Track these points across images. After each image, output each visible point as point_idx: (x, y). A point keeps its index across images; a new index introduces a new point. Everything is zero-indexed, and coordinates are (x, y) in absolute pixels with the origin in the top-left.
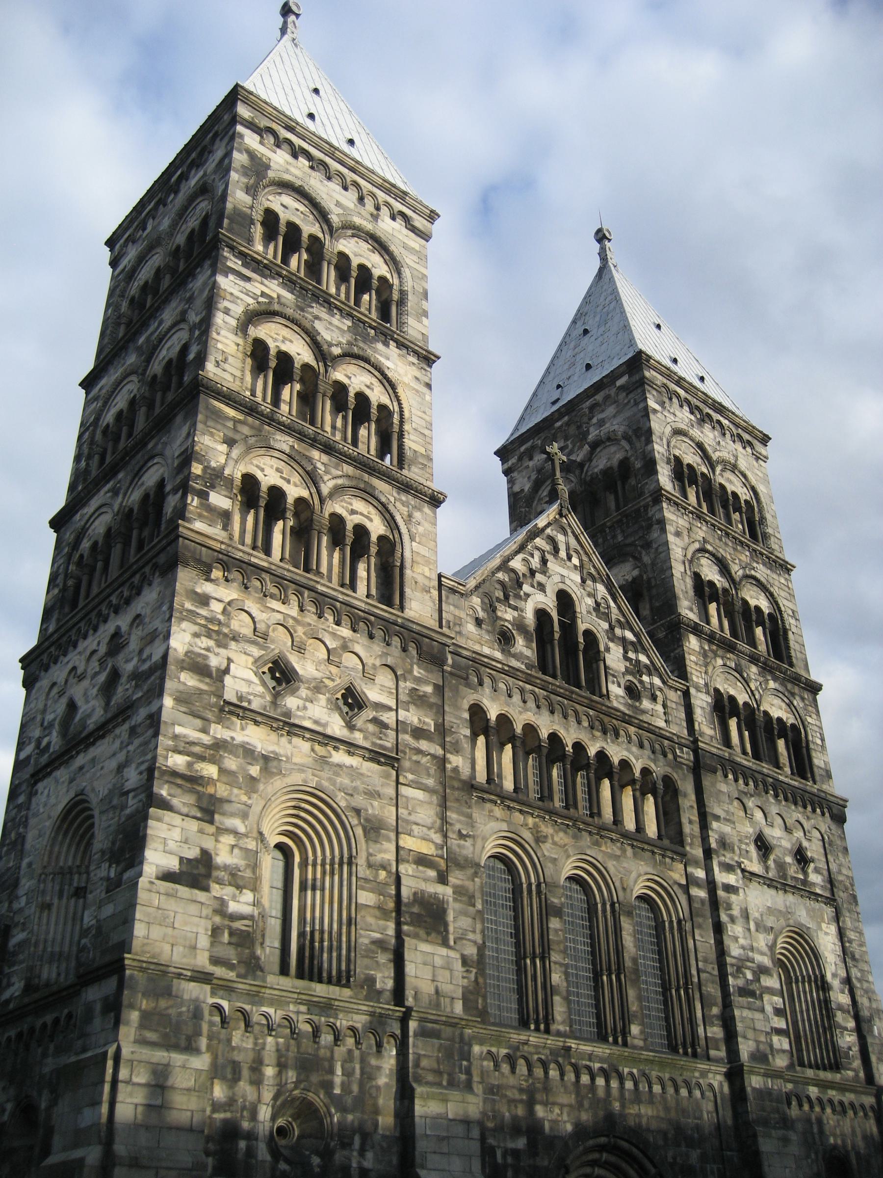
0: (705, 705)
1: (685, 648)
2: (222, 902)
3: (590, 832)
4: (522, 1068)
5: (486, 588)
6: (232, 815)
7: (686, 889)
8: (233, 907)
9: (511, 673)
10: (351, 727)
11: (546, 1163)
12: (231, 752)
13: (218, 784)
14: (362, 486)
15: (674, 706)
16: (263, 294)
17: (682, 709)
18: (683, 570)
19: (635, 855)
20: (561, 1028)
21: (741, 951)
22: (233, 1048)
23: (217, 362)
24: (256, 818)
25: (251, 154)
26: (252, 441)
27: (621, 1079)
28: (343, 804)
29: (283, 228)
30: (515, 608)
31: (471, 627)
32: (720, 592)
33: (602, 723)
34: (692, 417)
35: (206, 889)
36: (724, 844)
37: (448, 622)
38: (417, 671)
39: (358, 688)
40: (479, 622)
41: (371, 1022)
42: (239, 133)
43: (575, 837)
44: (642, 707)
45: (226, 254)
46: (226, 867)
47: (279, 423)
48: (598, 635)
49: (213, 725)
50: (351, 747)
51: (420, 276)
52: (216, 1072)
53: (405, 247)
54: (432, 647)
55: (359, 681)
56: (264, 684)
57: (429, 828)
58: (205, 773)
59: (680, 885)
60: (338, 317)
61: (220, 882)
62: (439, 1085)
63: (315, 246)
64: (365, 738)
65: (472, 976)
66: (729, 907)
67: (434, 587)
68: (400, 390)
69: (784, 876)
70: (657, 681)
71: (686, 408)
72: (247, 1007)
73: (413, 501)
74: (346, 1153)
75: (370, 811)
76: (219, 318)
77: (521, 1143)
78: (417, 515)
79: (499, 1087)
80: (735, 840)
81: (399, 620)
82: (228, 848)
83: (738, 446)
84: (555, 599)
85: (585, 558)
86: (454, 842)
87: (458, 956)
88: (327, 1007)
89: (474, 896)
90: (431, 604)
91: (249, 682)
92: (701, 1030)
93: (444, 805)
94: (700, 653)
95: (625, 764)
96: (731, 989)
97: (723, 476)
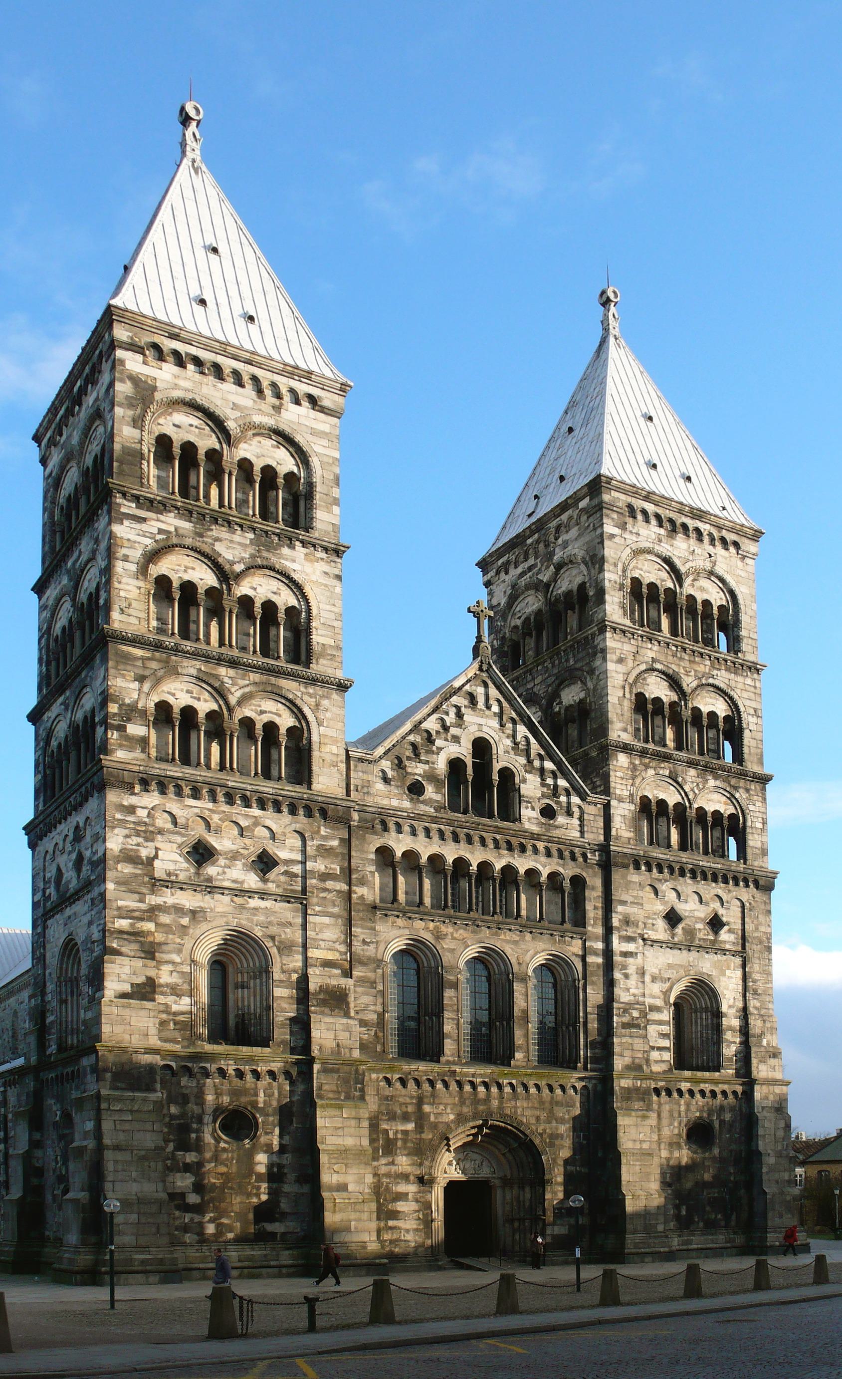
0: (626, 813)
1: (611, 767)
2: (167, 1005)
3: (489, 927)
4: (411, 1084)
5: (395, 752)
6: (169, 952)
7: (583, 958)
8: (175, 1008)
9: (419, 817)
10: (265, 881)
11: (430, 1136)
12: (164, 912)
13: (156, 934)
14: (269, 689)
15: (592, 818)
16: (160, 531)
17: (602, 820)
18: (621, 695)
19: (533, 938)
20: (451, 1059)
21: (632, 998)
22: (182, 1087)
23: (122, 610)
24: (189, 952)
25: (135, 380)
26: (161, 673)
27: (500, 1087)
28: (259, 934)
29: (177, 451)
30: (427, 762)
31: (380, 786)
32: (666, 706)
33: (509, 843)
34: (662, 531)
35: (153, 1000)
36: (627, 921)
37: (357, 786)
38: (323, 831)
39: (270, 852)
40: (386, 780)
41: (285, 1067)
42: (119, 360)
43: (473, 932)
44: (556, 823)
45: (119, 500)
46: (167, 985)
47: (187, 652)
48: (514, 770)
49: (147, 896)
50: (263, 895)
51: (331, 461)
52: (171, 1100)
53: (314, 432)
54: (338, 811)
55: (271, 846)
56: (187, 861)
57: (334, 942)
58: (145, 928)
59: (577, 955)
60: (239, 532)
61: (163, 994)
62: (338, 1099)
63: (214, 456)
64: (278, 886)
65: (373, 1033)
66: (624, 967)
67: (341, 762)
68: (307, 590)
69: (692, 939)
70: (575, 800)
71: (654, 522)
72: (190, 1065)
73: (320, 691)
74: (267, 1137)
75: (283, 936)
76: (119, 567)
77: (410, 1126)
78: (325, 703)
79: (392, 1096)
80: (641, 918)
81: (305, 796)
82: (169, 973)
83: (719, 550)
84: (471, 747)
85: (505, 704)
86: (357, 947)
87: (357, 1022)
88: (250, 1060)
89: (375, 982)
90: (339, 776)
91: (175, 862)
92: (582, 1053)
93: (349, 923)
94: (628, 768)
95: (532, 873)
96: (615, 1025)
97: (693, 586)
